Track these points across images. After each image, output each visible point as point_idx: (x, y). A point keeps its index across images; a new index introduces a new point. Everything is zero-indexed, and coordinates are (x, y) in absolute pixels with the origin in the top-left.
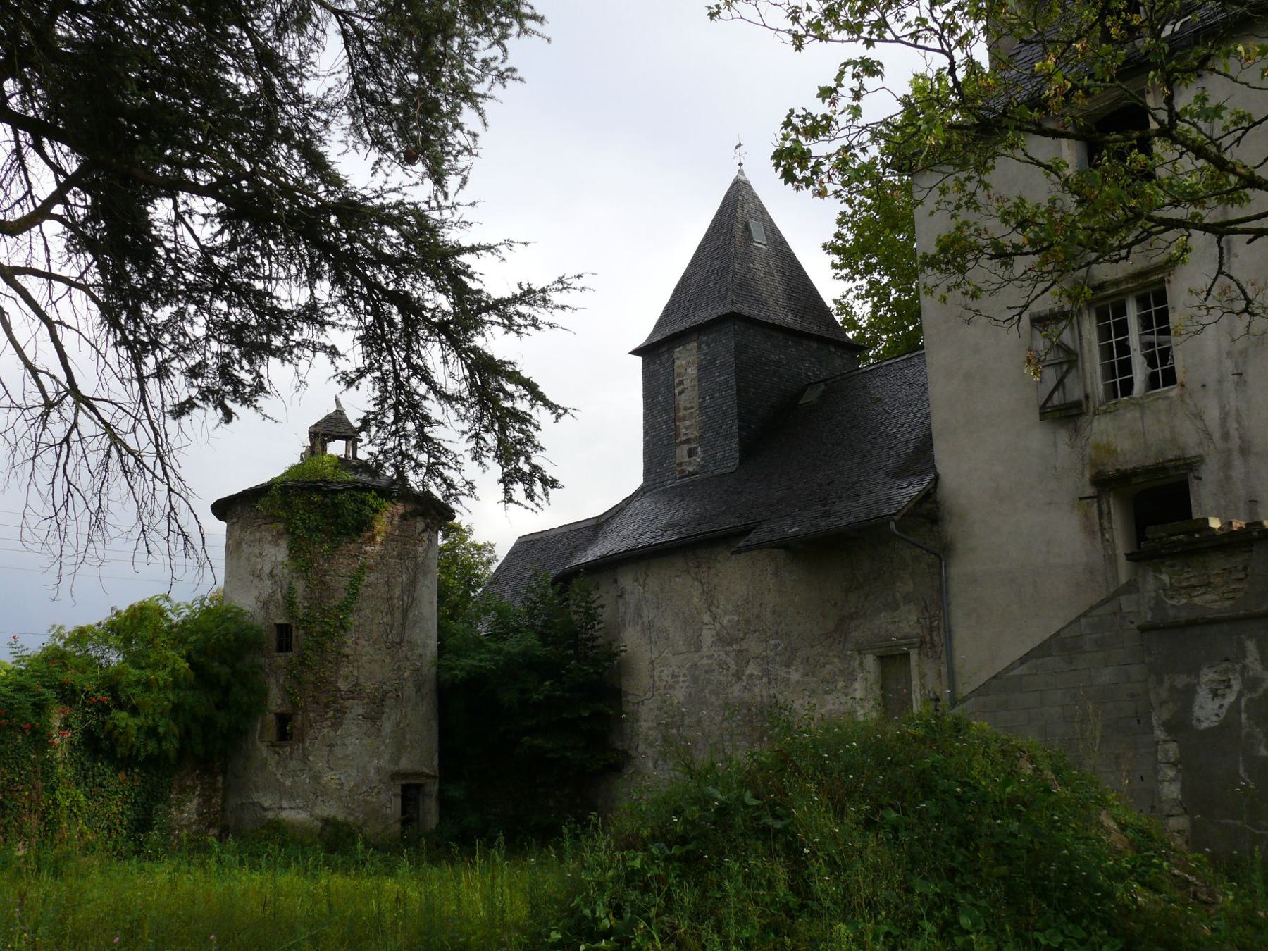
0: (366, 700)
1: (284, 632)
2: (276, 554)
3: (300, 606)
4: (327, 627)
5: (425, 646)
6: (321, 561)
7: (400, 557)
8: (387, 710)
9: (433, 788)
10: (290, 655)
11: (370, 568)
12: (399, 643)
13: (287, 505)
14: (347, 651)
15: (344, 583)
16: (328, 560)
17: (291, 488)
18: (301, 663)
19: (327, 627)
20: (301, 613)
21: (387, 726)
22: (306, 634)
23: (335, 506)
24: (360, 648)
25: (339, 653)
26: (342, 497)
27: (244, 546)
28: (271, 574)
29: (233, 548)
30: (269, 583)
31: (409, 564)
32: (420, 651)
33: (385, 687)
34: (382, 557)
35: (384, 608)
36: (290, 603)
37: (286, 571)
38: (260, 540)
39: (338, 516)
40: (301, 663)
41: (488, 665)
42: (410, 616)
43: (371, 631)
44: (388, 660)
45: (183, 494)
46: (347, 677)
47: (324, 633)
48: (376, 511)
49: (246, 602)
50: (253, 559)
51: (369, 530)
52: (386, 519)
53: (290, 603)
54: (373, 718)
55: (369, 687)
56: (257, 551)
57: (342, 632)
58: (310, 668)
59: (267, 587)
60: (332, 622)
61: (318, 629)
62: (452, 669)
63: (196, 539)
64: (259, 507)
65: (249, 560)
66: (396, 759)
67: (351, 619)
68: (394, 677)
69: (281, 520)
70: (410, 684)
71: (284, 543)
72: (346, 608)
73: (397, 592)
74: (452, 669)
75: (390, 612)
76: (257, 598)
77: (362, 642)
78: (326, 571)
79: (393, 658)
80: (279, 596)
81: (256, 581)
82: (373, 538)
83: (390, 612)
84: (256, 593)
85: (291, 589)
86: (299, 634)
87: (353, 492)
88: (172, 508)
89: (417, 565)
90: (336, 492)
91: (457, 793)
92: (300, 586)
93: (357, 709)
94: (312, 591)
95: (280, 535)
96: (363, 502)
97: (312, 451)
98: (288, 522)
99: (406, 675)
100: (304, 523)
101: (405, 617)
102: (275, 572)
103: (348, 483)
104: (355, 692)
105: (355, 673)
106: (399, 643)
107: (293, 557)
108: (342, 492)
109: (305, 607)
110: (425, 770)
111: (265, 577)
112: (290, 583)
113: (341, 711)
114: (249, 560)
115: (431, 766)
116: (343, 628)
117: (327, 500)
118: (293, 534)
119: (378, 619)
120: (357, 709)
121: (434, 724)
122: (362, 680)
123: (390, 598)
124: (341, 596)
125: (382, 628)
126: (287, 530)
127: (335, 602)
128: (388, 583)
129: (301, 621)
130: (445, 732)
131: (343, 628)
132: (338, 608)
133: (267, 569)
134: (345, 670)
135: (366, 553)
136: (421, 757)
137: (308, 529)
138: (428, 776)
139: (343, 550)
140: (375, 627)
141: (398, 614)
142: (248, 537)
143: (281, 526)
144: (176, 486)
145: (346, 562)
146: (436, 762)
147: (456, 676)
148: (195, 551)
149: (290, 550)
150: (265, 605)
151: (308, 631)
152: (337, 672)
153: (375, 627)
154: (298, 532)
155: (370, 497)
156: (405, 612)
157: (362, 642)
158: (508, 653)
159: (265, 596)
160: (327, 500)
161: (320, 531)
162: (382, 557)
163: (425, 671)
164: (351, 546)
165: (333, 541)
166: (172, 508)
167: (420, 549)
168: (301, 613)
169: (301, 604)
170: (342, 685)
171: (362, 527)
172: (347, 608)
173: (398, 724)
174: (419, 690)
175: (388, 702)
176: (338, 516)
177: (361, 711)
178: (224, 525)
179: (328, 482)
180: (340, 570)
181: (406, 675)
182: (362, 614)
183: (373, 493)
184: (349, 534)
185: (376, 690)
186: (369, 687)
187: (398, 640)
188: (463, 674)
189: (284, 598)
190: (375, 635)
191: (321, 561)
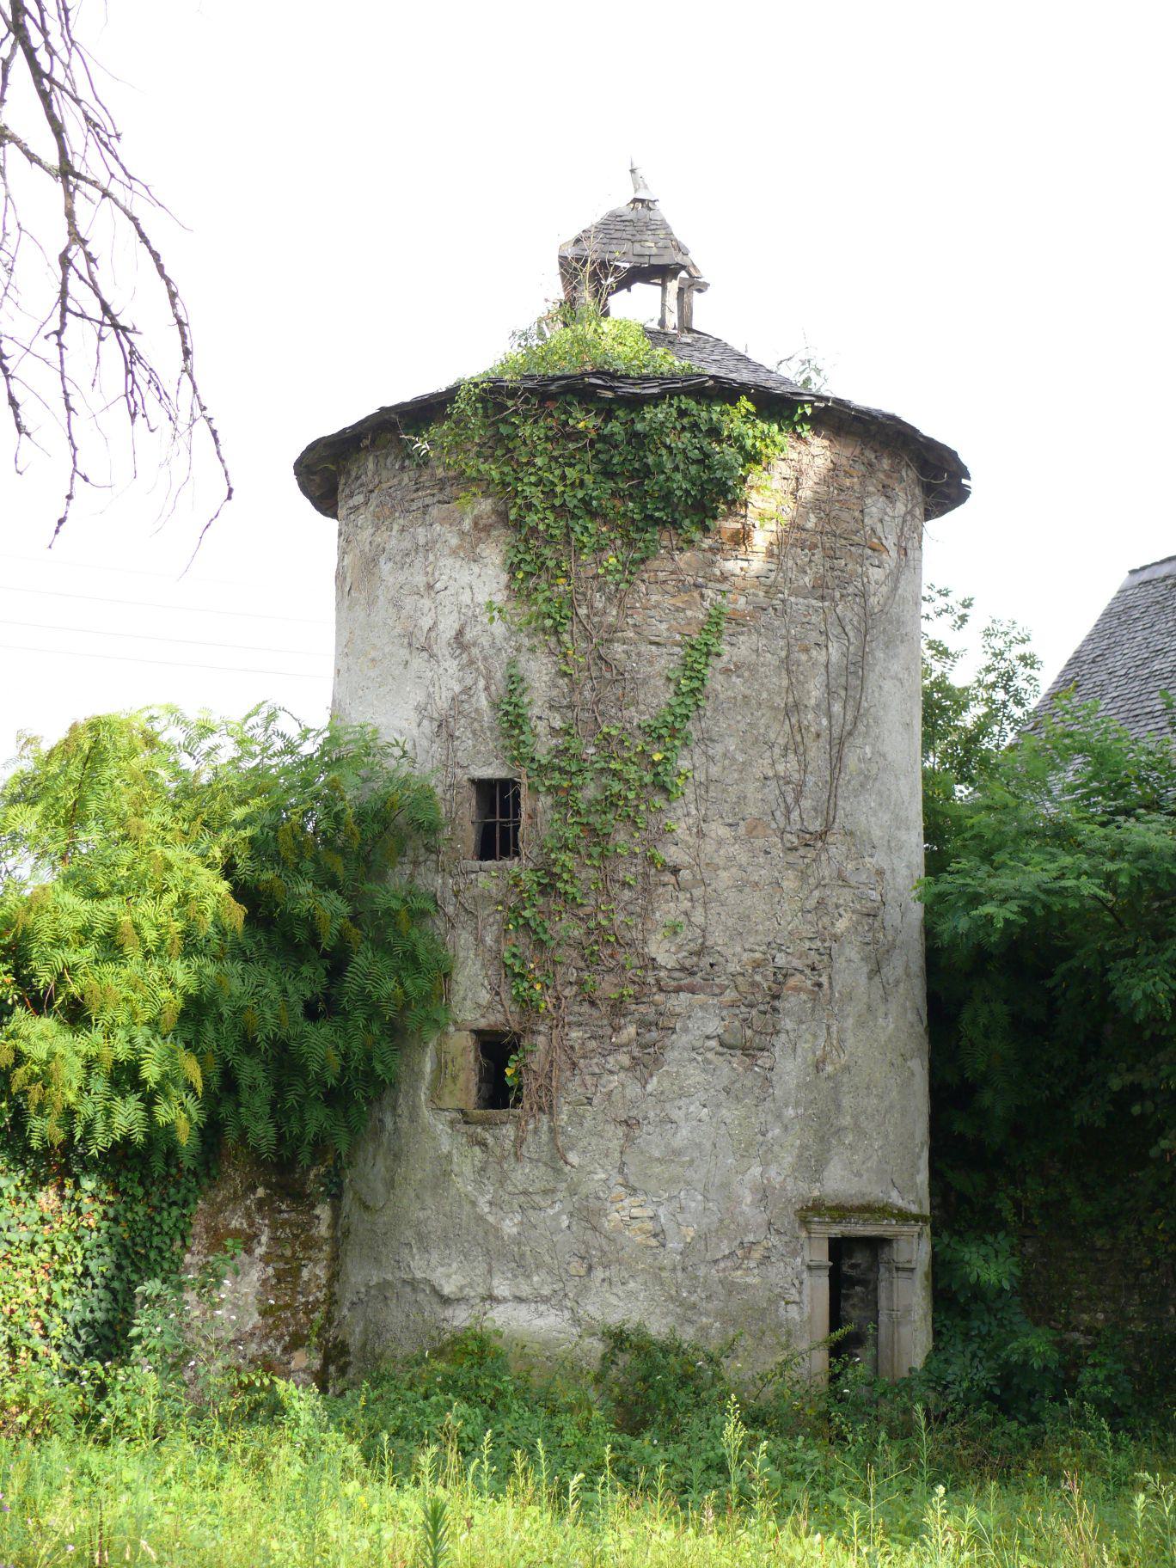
0: (730, 995)
1: (497, 800)
2: (471, 582)
3: (542, 728)
4: (617, 787)
5: (893, 847)
6: (599, 602)
7: (820, 590)
8: (788, 1024)
9: (916, 1250)
10: (512, 865)
11: (735, 619)
12: (822, 836)
13: (500, 444)
14: (672, 854)
15: (665, 662)
16: (617, 598)
17: (512, 393)
18: (544, 890)
19: (617, 787)
20: (543, 748)
21: (790, 1068)
22: (557, 806)
23: (637, 440)
24: (709, 847)
25: (651, 861)
26: (660, 413)
27: (385, 567)
28: (460, 642)
29: (356, 580)
30: (452, 665)
31: (848, 611)
32: (880, 860)
33: (781, 960)
34: (770, 590)
35: (779, 733)
36: (513, 721)
37: (499, 628)
38: (428, 547)
39: (647, 472)
40: (544, 890)
41: (1089, 887)
42: (852, 761)
43: (742, 798)
44: (790, 883)
45: (114, 188)
46: (674, 930)
47: (611, 802)
48: (753, 458)
49: (397, 721)
50: (409, 602)
51: (731, 514)
52: (783, 482)
53: (513, 721)
54: (746, 1048)
55: (736, 956)
56: (420, 580)
57: (659, 801)
58: (570, 900)
59: (448, 677)
60: (631, 772)
61: (591, 792)
62: (976, 900)
63: (159, 347)
64: (422, 445)
65: (397, 605)
66: (813, 1165)
67: (684, 764)
68: (807, 930)
69: (484, 484)
70: (852, 952)
71: (494, 555)
72: (668, 732)
73: (814, 691)
74: (976, 900)
75: (795, 747)
76: (420, 709)
77: (717, 829)
78: (613, 629)
79: (803, 876)
80: (484, 703)
81: (418, 662)
82: (742, 538)
83: (795, 747)
84: (419, 697)
85: (515, 682)
86: (536, 807)
87: (688, 403)
88: (76, 237)
89: (867, 616)
90: (636, 403)
91: (989, 1267)
92: (539, 672)
93: (702, 1020)
94: (574, 686)
95: (482, 529)
96: (714, 432)
97: (569, 310)
98: (505, 490)
99: (841, 925)
100: (550, 494)
101: (836, 762)
102: (469, 636)
103: (674, 378)
104: (697, 972)
105: (698, 918)
106: (822, 836)
107: (520, 591)
108: (655, 400)
109: (554, 732)
110: (896, 1199)
111: (442, 649)
112: (512, 664)
113: (660, 1025)
114: (397, 605)
115: (912, 1189)
116: (664, 789)
117: (614, 427)
118: (518, 524)
119: (762, 767)
120: (702, 1020)
121: (919, 1069)
122: (717, 938)
123: (796, 707)
124: (656, 699)
125: (772, 788)
126: (503, 516)
127: (638, 716)
128: (787, 665)
129: (543, 770)
130: (950, 1096)
131: (664, 789)
132: (648, 731)
133: (448, 626)
134: (668, 909)
135: (724, 578)
136: (883, 1159)
137: (561, 511)
138: (904, 1217)
139: (660, 566)
140: (751, 789)
141: (817, 754)
142: (393, 540)
143: (485, 506)
144: (87, 159)
145: (668, 601)
146: (923, 1177)
147: (989, 919)
148: (162, 396)
149: (513, 569)
150: (444, 729)
151: (564, 801)
152: (645, 914)
153: (751, 789)
154: (532, 519)
155: (737, 419)
156: (838, 746)
157: (717, 829)
158: (1144, 853)
159: (442, 702)
160: (614, 427)
161: (593, 515)
162: (770, 590)
163: (892, 916)
164: (685, 558)
165: (630, 544)
166: (76, 237)
167: (876, 574)
168: (543, 748)
169: (544, 725)
170: (662, 951)
171: (710, 499)
172: (674, 733)
173: (818, 1066)
174: (876, 971)
175: (790, 1002)
176: (647, 472)
177: (714, 1026)
178: (332, 525)
179: (613, 376)
180: (653, 619)
181: (841, 925)
182: (717, 750)
183: (745, 404)
184: (676, 524)
185: (757, 965)
186: (736, 956)
187: (816, 826)
188: (1010, 912)
189: (495, 706)
190: (752, 810)
191: (599, 602)
